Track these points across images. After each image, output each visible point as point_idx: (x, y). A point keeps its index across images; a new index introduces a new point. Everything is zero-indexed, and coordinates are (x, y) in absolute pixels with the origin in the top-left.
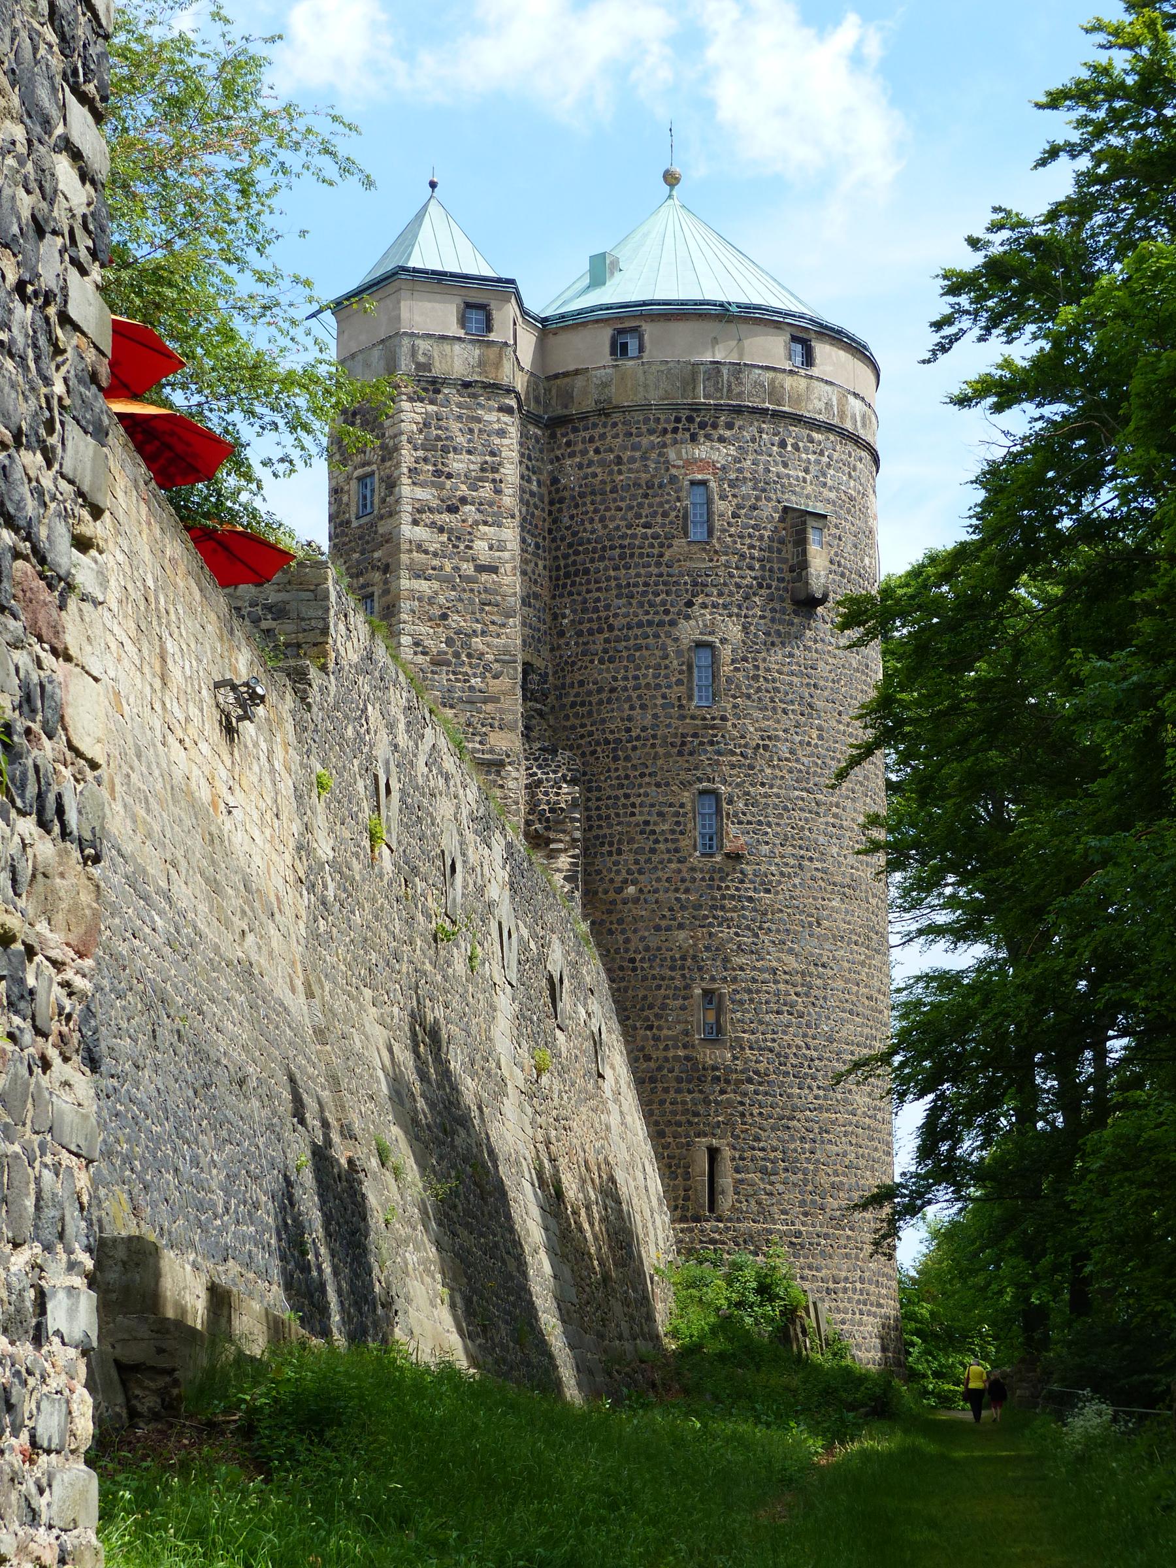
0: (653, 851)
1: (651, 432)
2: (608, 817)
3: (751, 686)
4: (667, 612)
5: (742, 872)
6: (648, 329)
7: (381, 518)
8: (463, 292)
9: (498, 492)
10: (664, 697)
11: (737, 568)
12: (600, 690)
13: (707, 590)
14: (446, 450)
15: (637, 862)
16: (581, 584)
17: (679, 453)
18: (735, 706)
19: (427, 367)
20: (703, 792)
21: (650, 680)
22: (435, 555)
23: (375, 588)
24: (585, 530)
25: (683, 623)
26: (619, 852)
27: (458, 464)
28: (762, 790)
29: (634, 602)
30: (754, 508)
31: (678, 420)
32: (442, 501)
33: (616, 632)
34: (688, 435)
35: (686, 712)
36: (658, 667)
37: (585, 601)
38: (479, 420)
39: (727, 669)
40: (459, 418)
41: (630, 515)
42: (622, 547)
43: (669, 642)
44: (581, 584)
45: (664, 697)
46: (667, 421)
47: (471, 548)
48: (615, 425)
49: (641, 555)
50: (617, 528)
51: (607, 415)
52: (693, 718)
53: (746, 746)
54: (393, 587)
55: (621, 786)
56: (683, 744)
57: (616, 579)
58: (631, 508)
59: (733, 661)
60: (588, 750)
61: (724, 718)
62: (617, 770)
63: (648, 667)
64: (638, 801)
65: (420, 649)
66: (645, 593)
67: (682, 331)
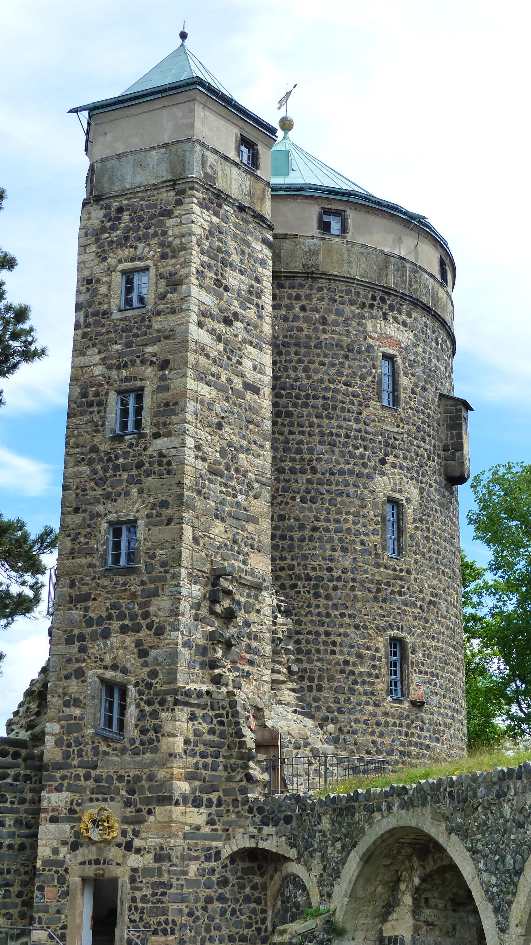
0: (352, 691)
1: (352, 303)
2: (309, 652)
3: (424, 546)
4: (365, 465)
5: (423, 721)
6: (352, 216)
7: (159, 313)
8: (241, 124)
9: (260, 317)
10: (363, 543)
11: (415, 438)
12: (302, 527)
13: (397, 451)
14: (225, 263)
15: (337, 701)
16: (283, 425)
17: (374, 326)
18: (416, 562)
21: (350, 525)
22: (214, 362)
23: (147, 383)
24: (288, 377)
26: (320, 689)
27: (233, 279)
28: (434, 643)
29: (337, 450)
30: (424, 389)
31: (374, 298)
32: (221, 311)
33: (319, 475)
35: (380, 561)
37: (287, 441)
39: (410, 527)
40: (235, 236)
41: (332, 371)
42: (324, 398)
43: (366, 492)
44: (283, 425)
45: (363, 543)
46: (365, 297)
47: (240, 364)
48: (320, 289)
49: (343, 409)
50: (321, 381)
51: (314, 279)
53: (423, 600)
54: (175, 384)
56: (379, 590)
57: (319, 426)
58: (334, 365)
59: (414, 520)
60: (288, 583)
61: (408, 572)
62: (318, 606)
63: (348, 513)
64: (338, 640)
65: (200, 454)
66: (345, 445)
67: (378, 223)
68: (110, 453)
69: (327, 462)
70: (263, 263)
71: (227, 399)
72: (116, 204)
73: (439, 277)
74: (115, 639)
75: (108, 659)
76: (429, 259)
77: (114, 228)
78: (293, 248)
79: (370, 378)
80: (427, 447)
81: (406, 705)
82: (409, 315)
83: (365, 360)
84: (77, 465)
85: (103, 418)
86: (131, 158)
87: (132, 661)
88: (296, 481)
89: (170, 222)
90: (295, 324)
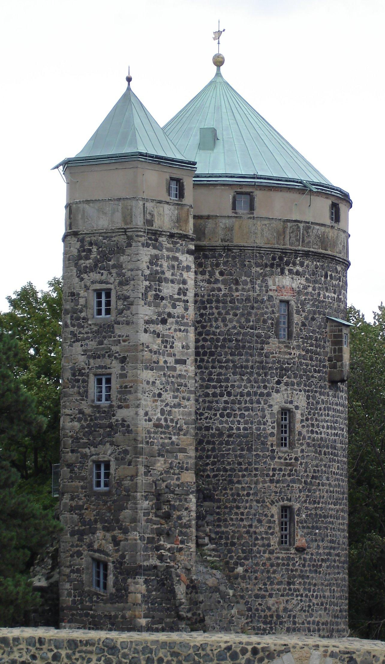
4: (265, 387)
9: (186, 309)
14: (160, 281)
16: (208, 362)
18: (302, 451)
19: (150, 222)
20: (284, 509)
22: (155, 353)
25: (274, 395)
27: (168, 289)
31: (274, 259)
33: (232, 398)
34: (279, 270)
36: (259, 423)
37: (210, 374)
38: (176, 259)
39: (298, 426)
42: (237, 340)
44: (208, 362)
49: (250, 348)
50: (234, 327)
52: (280, 458)
55: (235, 500)
56: (274, 475)
57: (233, 361)
59: (302, 421)
65: (147, 418)
68: (91, 416)
69: (239, 387)
70: (188, 268)
72: (89, 239)
73: (328, 222)
74: (100, 534)
75: (96, 547)
76: (320, 210)
77: (87, 258)
78: (214, 226)
79: (270, 321)
80: (314, 363)
81: (293, 551)
83: (267, 308)
84: (71, 422)
85: (86, 391)
86: (97, 205)
87: (111, 547)
88: (217, 402)
89: (123, 258)
90: (216, 286)
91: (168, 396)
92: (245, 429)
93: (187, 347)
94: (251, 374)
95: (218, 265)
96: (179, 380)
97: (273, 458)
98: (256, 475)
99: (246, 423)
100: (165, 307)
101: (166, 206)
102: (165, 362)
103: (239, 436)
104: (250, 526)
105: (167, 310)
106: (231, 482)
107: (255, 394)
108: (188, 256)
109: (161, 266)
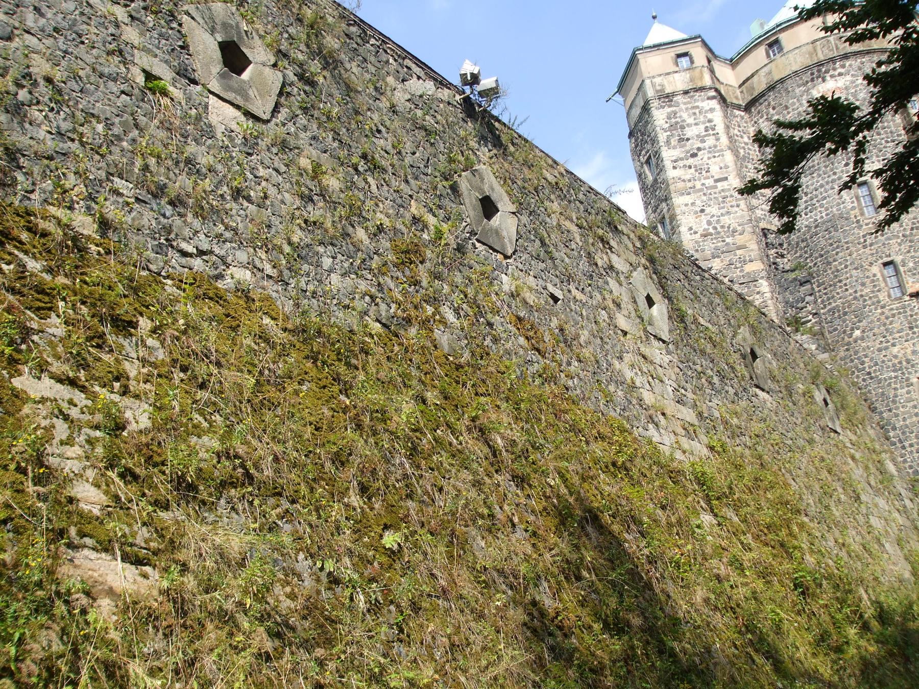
4: (835, 174)
9: (718, 139)
14: (683, 128)
19: (663, 90)
22: (690, 181)
27: (690, 132)
31: (812, 74)
34: (820, 80)
36: (838, 204)
38: (697, 107)
70: (712, 110)
71: (704, 194)
82: (843, 66)
91: (713, 210)
92: (827, 215)
93: (727, 167)
94: (819, 169)
95: (769, 105)
96: (723, 194)
97: (860, 227)
98: (848, 248)
99: (827, 209)
100: (692, 144)
101: (676, 75)
102: (703, 184)
103: (824, 223)
104: (856, 292)
105: (696, 146)
106: (829, 263)
107: (827, 183)
108: (709, 101)
109: (680, 117)
